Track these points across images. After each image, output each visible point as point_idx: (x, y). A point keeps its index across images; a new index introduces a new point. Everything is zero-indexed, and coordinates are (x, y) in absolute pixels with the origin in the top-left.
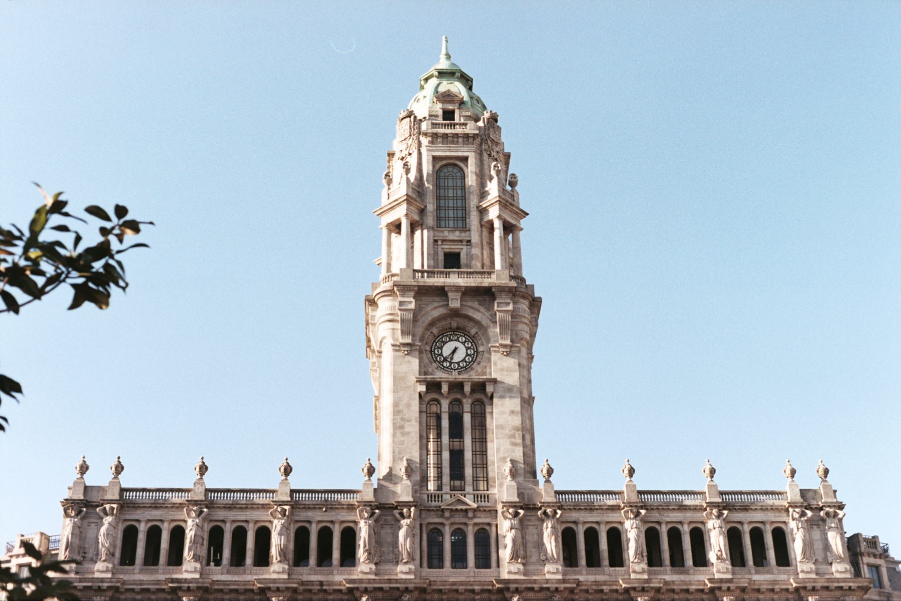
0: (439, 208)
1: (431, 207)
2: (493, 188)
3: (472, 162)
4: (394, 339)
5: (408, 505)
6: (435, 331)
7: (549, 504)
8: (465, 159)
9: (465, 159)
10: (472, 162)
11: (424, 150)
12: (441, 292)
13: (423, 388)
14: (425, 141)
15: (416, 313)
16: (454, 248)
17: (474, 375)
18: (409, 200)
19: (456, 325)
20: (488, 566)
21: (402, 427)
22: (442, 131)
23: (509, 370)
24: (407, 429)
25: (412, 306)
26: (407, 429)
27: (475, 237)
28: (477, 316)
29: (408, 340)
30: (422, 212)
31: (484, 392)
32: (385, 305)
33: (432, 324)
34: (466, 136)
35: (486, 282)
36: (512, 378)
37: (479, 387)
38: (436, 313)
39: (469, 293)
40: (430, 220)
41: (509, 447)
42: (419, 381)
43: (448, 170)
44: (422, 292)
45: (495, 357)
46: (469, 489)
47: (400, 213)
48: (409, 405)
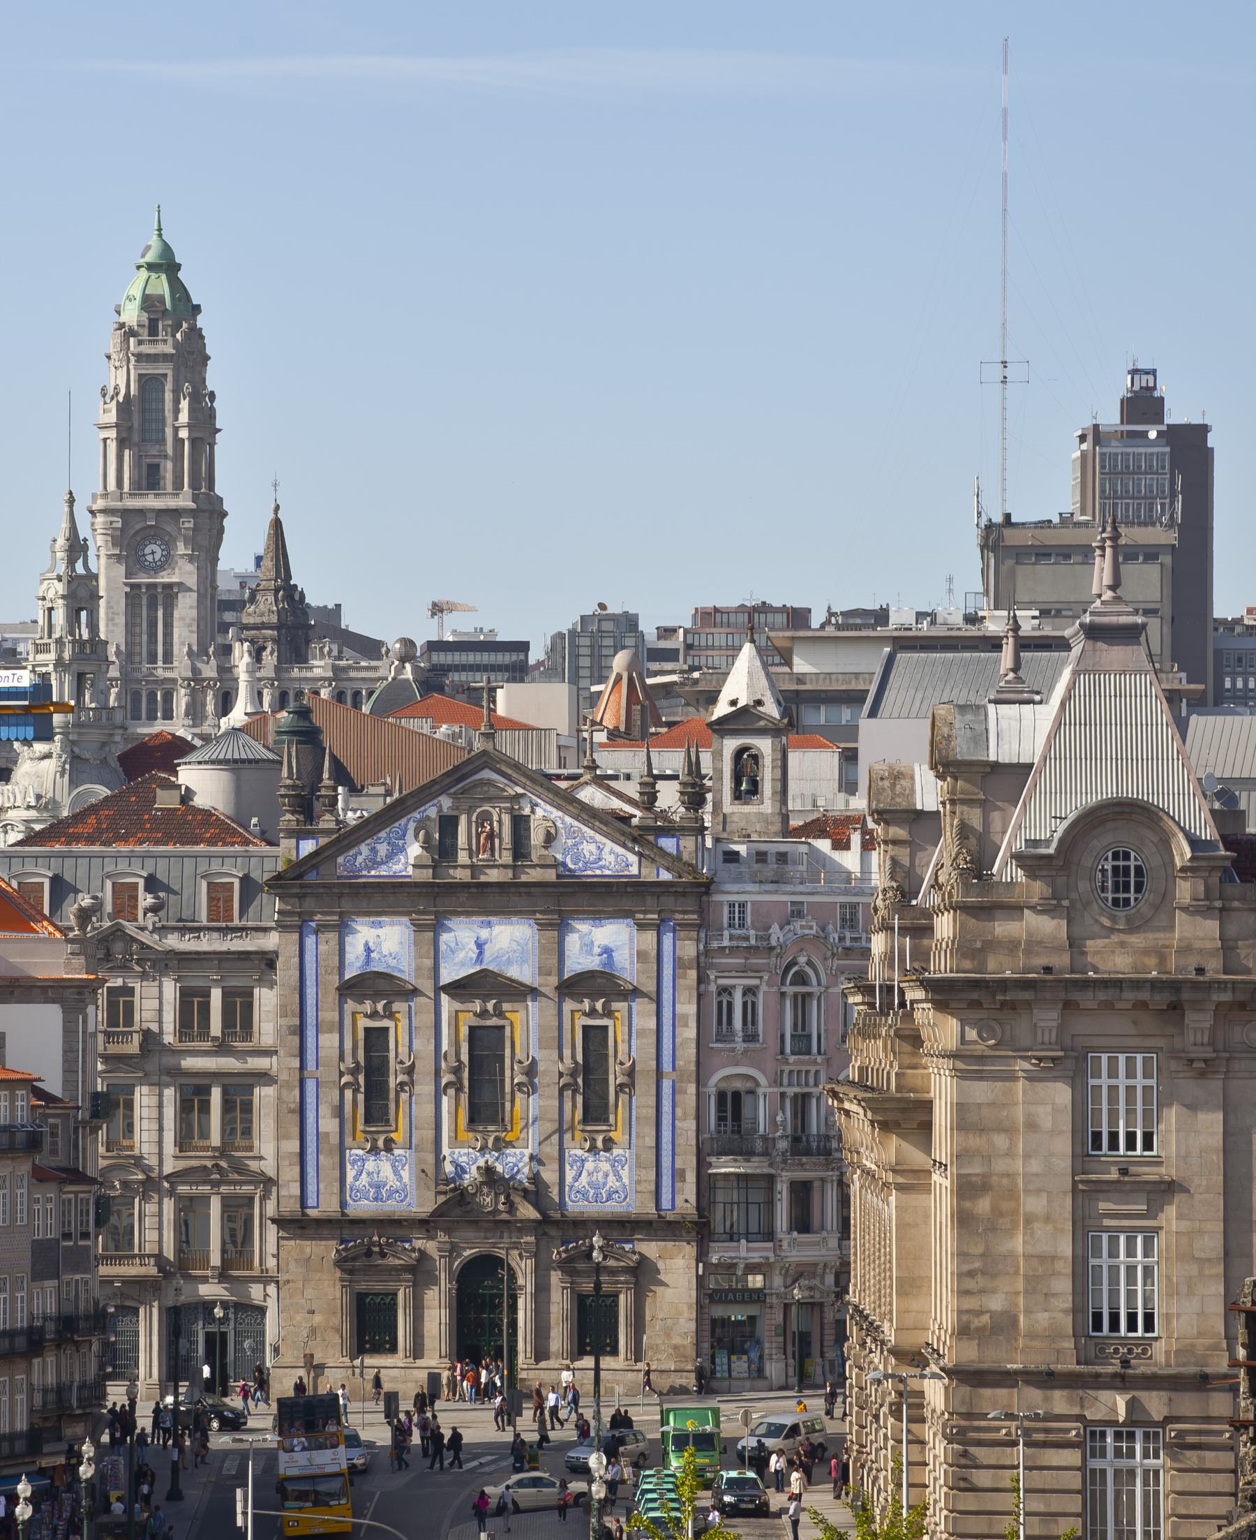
0: (144, 421)
1: (136, 425)
2: (184, 417)
3: (170, 378)
4: (108, 550)
5: (116, 679)
6: (138, 539)
7: (210, 679)
8: (165, 375)
9: (165, 375)
10: (170, 378)
11: (131, 367)
12: (141, 512)
13: (128, 589)
14: (132, 359)
15: (122, 530)
16: (156, 461)
17: (164, 578)
18: (117, 426)
19: (154, 534)
20: (171, 718)
21: (112, 619)
22: (147, 349)
23: (189, 573)
24: (117, 621)
25: (119, 525)
26: (117, 621)
27: (170, 451)
28: (169, 528)
29: (117, 552)
30: (130, 429)
31: (170, 593)
32: (100, 519)
33: (137, 532)
34: (165, 357)
35: (172, 503)
36: (192, 581)
37: (168, 587)
38: (138, 527)
39: (160, 512)
40: (136, 437)
41: (188, 634)
42: (126, 584)
43: (150, 384)
44: (125, 513)
45: (181, 562)
46: (160, 663)
47: (112, 434)
48: (118, 603)
